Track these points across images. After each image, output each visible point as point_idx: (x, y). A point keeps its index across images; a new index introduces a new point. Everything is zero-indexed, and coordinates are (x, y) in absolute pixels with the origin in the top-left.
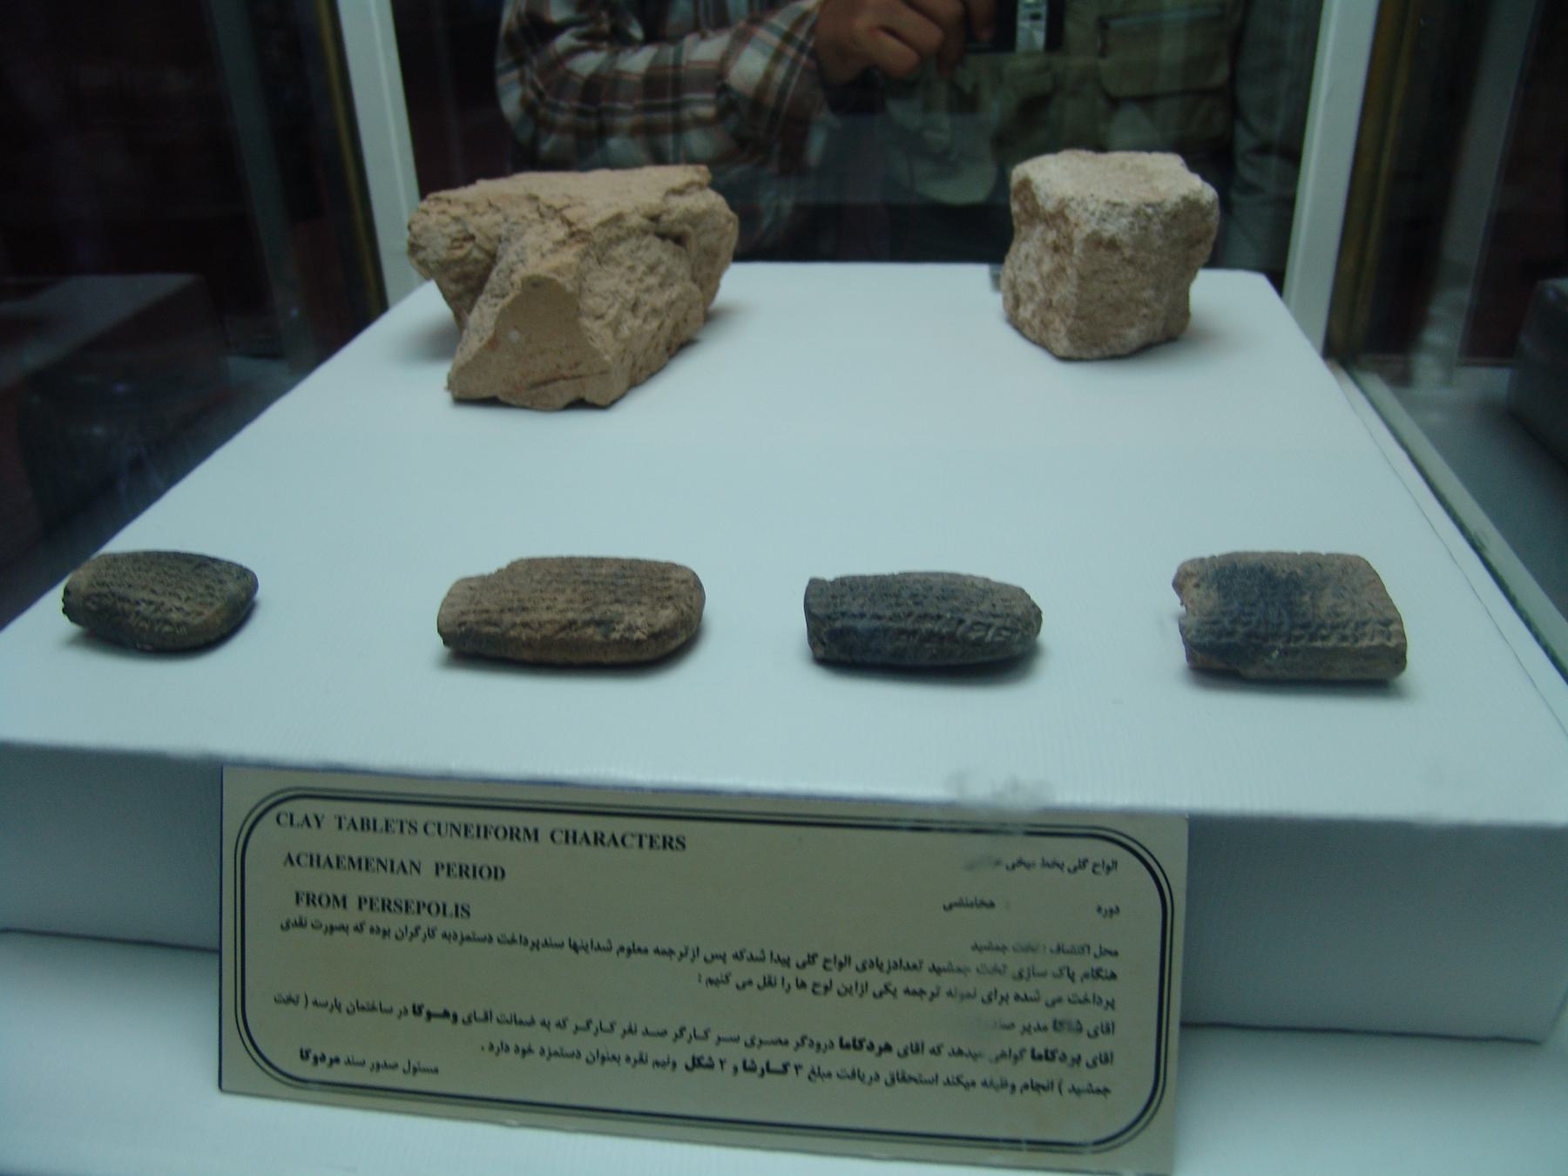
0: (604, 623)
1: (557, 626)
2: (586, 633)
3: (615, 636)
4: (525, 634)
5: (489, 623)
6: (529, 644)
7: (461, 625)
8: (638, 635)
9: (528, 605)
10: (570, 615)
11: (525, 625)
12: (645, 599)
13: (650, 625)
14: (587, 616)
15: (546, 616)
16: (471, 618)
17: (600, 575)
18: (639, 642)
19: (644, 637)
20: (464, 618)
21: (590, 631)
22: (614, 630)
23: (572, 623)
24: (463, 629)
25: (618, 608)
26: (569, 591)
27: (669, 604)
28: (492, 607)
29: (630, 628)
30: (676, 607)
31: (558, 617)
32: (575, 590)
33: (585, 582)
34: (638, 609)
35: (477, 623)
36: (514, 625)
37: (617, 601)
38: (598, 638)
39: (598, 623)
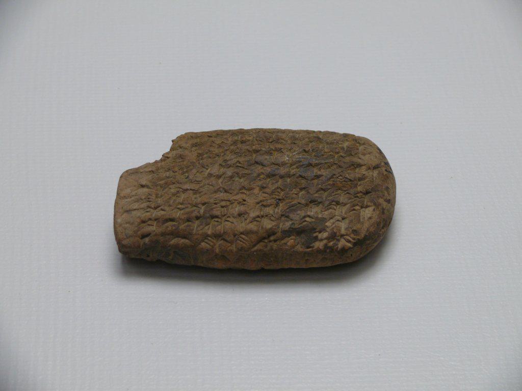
0: (306, 232)
1: (254, 238)
2: (285, 244)
3: (319, 245)
4: (218, 245)
5: (175, 234)
6: (223, 257)
7: (144, 236)
8: (342, 243)
9: (216, 212)
10: (268, 224)
11: (218, 236)
12: (343, 198)
13: (355, 232)
14: (288, 224)
15: (241, 226)
16: (153, 228)
17: (283, 164)
18: (344, 250)
19: (349, 245)
20: (147, 229)
21: (290, 241)
22: (316, 238)
23: (271, 233)
24: (147, 240)
25: (314, 211)
26: (256, 191)
27: (366, 200)
28: (178, 214)
29: (333, 236)
30: (377, 205)
31: (253, 227)
32: (262, 188)
33: (271, 176)
34: (340, 211)
35: (163, 234)
36: (206, 236)
37: (313, 201)
38: (299, 248)
39: (299, 232)
